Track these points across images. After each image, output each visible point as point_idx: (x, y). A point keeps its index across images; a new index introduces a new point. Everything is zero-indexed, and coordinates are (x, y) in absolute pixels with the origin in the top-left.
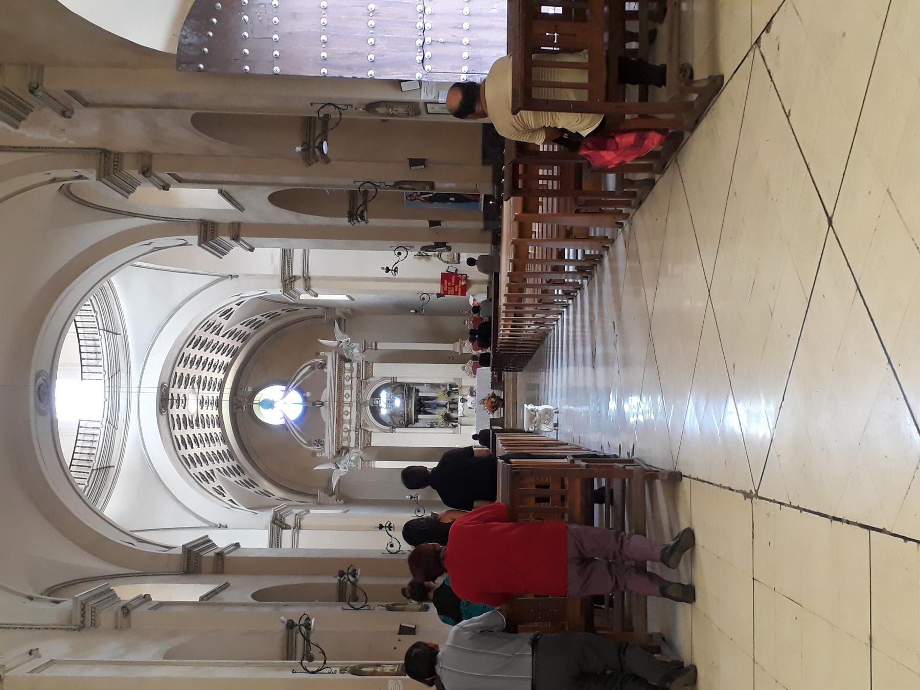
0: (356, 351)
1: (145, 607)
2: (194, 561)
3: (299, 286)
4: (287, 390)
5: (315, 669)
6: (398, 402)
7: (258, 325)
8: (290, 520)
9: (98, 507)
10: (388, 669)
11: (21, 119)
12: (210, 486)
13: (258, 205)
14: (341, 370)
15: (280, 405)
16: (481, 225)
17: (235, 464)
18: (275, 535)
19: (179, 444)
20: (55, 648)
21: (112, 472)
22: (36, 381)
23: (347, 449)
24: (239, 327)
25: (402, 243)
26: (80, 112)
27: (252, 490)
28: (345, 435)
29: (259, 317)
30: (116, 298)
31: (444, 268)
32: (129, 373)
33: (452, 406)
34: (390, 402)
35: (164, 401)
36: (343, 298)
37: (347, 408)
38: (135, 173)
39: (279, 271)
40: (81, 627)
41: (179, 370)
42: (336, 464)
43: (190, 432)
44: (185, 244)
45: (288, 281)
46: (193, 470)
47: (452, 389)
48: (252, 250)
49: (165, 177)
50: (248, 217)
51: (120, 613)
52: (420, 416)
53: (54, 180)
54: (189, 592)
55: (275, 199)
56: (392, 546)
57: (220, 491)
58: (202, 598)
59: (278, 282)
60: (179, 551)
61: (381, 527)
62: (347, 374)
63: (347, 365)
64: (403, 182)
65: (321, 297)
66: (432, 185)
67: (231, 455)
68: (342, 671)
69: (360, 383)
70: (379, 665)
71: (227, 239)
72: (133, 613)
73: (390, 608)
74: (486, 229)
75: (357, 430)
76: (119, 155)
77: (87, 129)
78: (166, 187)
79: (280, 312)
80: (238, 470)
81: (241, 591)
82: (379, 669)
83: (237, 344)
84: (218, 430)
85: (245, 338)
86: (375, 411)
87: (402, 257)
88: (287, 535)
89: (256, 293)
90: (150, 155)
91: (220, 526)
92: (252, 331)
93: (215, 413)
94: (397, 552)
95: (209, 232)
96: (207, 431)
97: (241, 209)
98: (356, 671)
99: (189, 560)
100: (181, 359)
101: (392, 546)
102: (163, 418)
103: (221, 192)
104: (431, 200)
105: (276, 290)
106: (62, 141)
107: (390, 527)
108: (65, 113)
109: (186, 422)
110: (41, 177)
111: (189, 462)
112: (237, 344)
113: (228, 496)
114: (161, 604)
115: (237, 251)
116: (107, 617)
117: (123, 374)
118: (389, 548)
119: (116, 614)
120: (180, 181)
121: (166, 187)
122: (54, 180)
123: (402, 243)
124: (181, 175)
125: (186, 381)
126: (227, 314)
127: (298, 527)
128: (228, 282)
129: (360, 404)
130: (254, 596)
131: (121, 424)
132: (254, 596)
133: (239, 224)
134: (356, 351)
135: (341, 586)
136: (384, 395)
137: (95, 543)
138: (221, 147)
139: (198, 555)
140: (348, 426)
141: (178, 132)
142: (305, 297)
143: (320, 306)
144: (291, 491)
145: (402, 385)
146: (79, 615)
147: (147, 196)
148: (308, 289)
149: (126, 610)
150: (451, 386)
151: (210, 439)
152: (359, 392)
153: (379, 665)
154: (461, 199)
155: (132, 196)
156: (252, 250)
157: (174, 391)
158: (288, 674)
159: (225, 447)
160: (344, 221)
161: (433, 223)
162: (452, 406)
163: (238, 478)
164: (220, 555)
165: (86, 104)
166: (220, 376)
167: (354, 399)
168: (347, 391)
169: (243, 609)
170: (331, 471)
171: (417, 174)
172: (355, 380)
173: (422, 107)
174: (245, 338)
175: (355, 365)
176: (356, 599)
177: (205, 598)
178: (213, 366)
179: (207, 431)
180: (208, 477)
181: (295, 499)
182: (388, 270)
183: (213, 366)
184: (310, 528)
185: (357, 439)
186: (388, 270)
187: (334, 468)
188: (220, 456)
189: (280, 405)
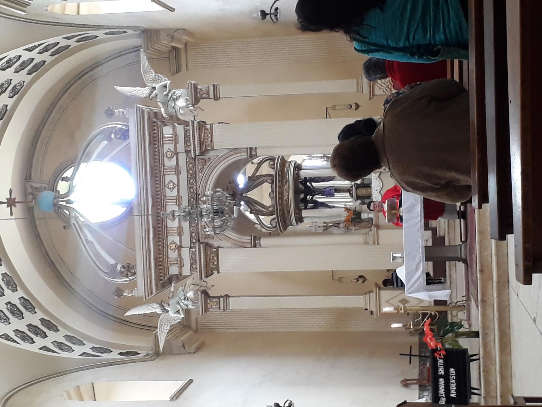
0: (181, 103)
28: (173, 254)
33: (363, 192)
42: (162, 306)
52: (305, 213)
69: (192, 162)
79: (72, 43)
134: (181, 103)
140: (177, 239)
143: (129, 27)
152: (192, 177)
162: (363, 192)
163: (16, 324)
168: (171, 177)
170: (156, 316)
172: (182, 157)
175: (180, 129)
187: (158, 310)
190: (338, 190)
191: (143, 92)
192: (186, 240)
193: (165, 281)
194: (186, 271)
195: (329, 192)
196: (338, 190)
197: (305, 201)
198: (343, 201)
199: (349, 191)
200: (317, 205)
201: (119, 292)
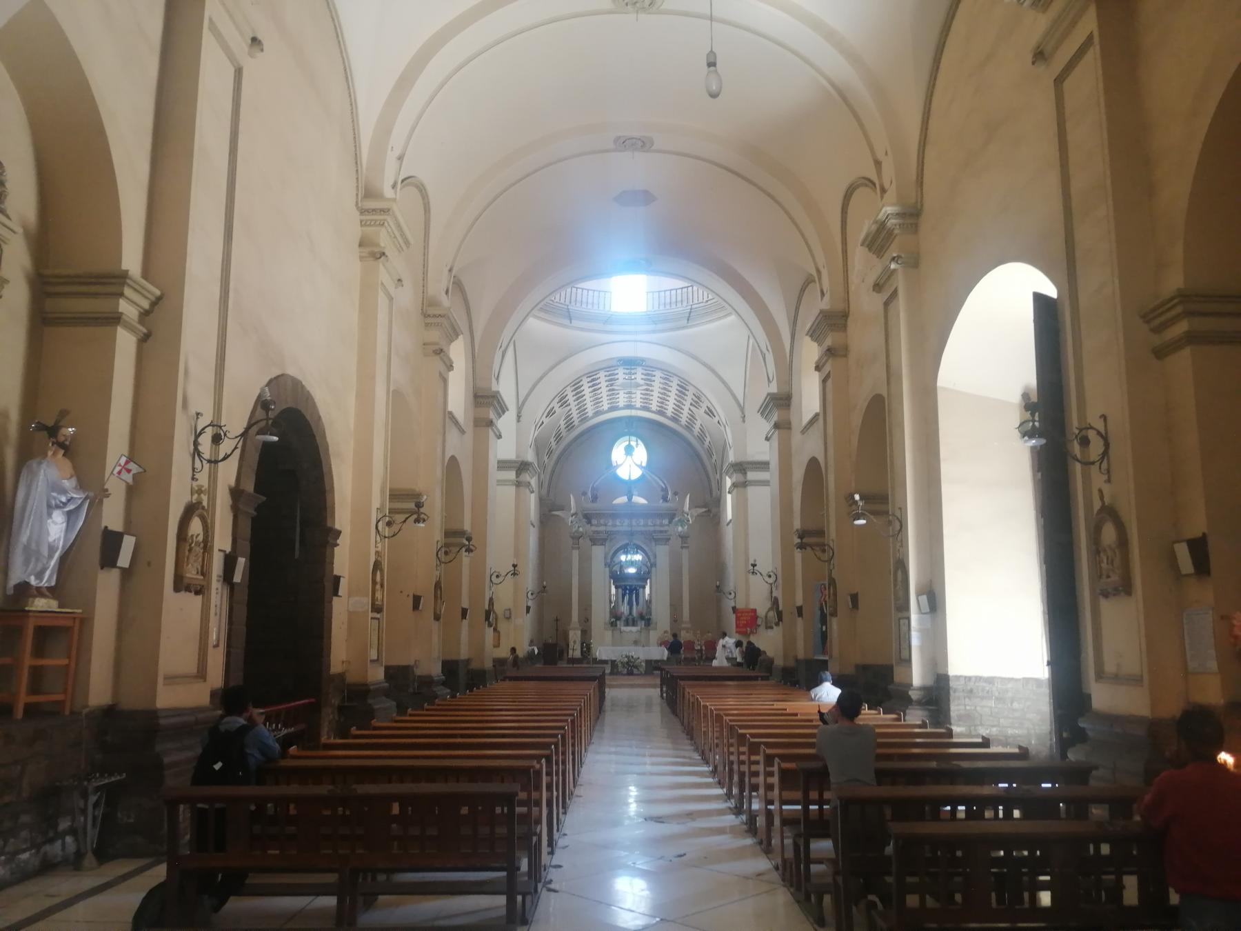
1: (443, 368)
2: (485, 401)
3: (737, 477)
4: (640, 466)
5: (380, 528)
6: (632, 570)
7: (701, 439)
8: (526, 477)
9: (535, 312)
10: (378, 595)
11: (870, 247)
12: (555, 405)
13: (809, 447)
14: (661, 516)
15: (629, 461)
16: (801, 655)
17: (576, 423)
19: (592, 375)
20: (406, 297)
21: (567, 322)
23: (589, 522)
24: (698, 423)
25: (780, 581)
26: (879, 299)
27: (552, 440)
28: (602, 521)
29: (708, 439)
30: (720, 318)
31: (761, 612)
32: (654, 332)
34: (632, 563)
35: (630, 363)
36: (729, 514)
37: (627, 522)
38: (828, 342)
39: (750, 459)
40: (425, 315)
41: (658, 374)
42: (575, 514)
43: (603, 385)
44: (769, 381)
45: (740, 468)
46: (569, 389)
47: (646, 619)
48: (767, 439)
49: (828, 368)
50: (796, 437)
51: (436, 347)
53: (818, 271)
54: (457, 399)
55: (813, 464)
57: (551, 413)
58: (450, 413)
59: (739, 460)
60: (494, 388)
61: (515, 566)
62: (658, 522)
63: (666, 522)
64: (835, 588)
65: (729, 497)
66: (834, 614)
67: (584, 419)
68: (377, 552)
70: (382, 586)
71: (775, 418)
72: (437, 357)
73: (438, 586)
74: (797, 660)
75: (607, 532)
76: (844, 328)
77: (866, 303)
78: (818, 368)
79: (715, 457)
80: (570, 426)
81: (457, 445)
82: (378, 587)
83: (684, 420)
84: (606, 407)
85: (689, 428)
86: (625, 549)
87: (767, 579)
88: (511, 475)
89: (730, 440)
90: (845, 356)
91: (519, 417)
92: (696, 433)
93: (621, 404)
95: (782, 401)
96: (605, 399)
97: (803, 432)
98: (377, 566)
99: (487, 397)
100: (668, 375)
102: (615, 363)
103: (817, 415)
104: (821, 609)
105: (732, 457)
106: (854, 279)
108: (878, 287)
109: (611, 380)
110: (821, 261)
111: (576, 386)
112: (684, 420)
113: (546, 421)
114: (445, 381)
115: (765, 426)
116: (434, 335)
117: (652, 327)
119: (437, 344)
120: (824, 381)
121: (818, 368)
122: (818, 271)
123: (780, 581)
124: (829, 382)
125: (649, 379)
126: (710, 412)
127: (518, 484)
128: (739, 413)
129: (632, 534)
130: (453, 458)
131: (609, 328)
132: (453, 458)
133: (790, 428)
134: (680, 529)
135: (462, 533)
136: (638, 557)
137: (500, 316)
138: (857, 420)
141: (869, 383)
142: (728, 482)
144: (553, 471)
145: (649, 572)
146: (437, 313)
147: (810, 351)
148: (734, 485)
149: (440, 352)
150: (649, 620)
151: (597, 401)
152: (642, 533)
153: (382, 586)
154: (824, 636)
155: (808, 339)
156: (767, 439)
157: (639, 370)
158: (376, 503)
159: (590, 414)
160: (797, 524)
161: (800, 611)
163: (563, 427)
164: (490, 423)
165: (886, 304)
166: (654, 408)
167: (634, 529)
169: (439, 450)
171: (844, 602)
172: (652, 529)
173: (904, 614)
174: (689, 428)
175: (666, 528)
176: (446, 553)
177: (451, 416)
178: (663, 400)
179: (605, 399)
180: (563, 402)
181: (546, 478)
182: (754, 565)
183: (663, 400)
184: (517, 492)
185: (598, 532)
186: (754, 565)
187: (573, 511)
188: (582, 410)
189: (629, 461)
190: (631, 609)
191: (686, 508)
192: (609, 529)
193: (588, 518)
194: (594, 528)
195: (630, 603)
196: (631, 609)
197: (625, 589)
198: (624, 609)
199: (631, 613)
200: (623, 596)
201: (584, 494)
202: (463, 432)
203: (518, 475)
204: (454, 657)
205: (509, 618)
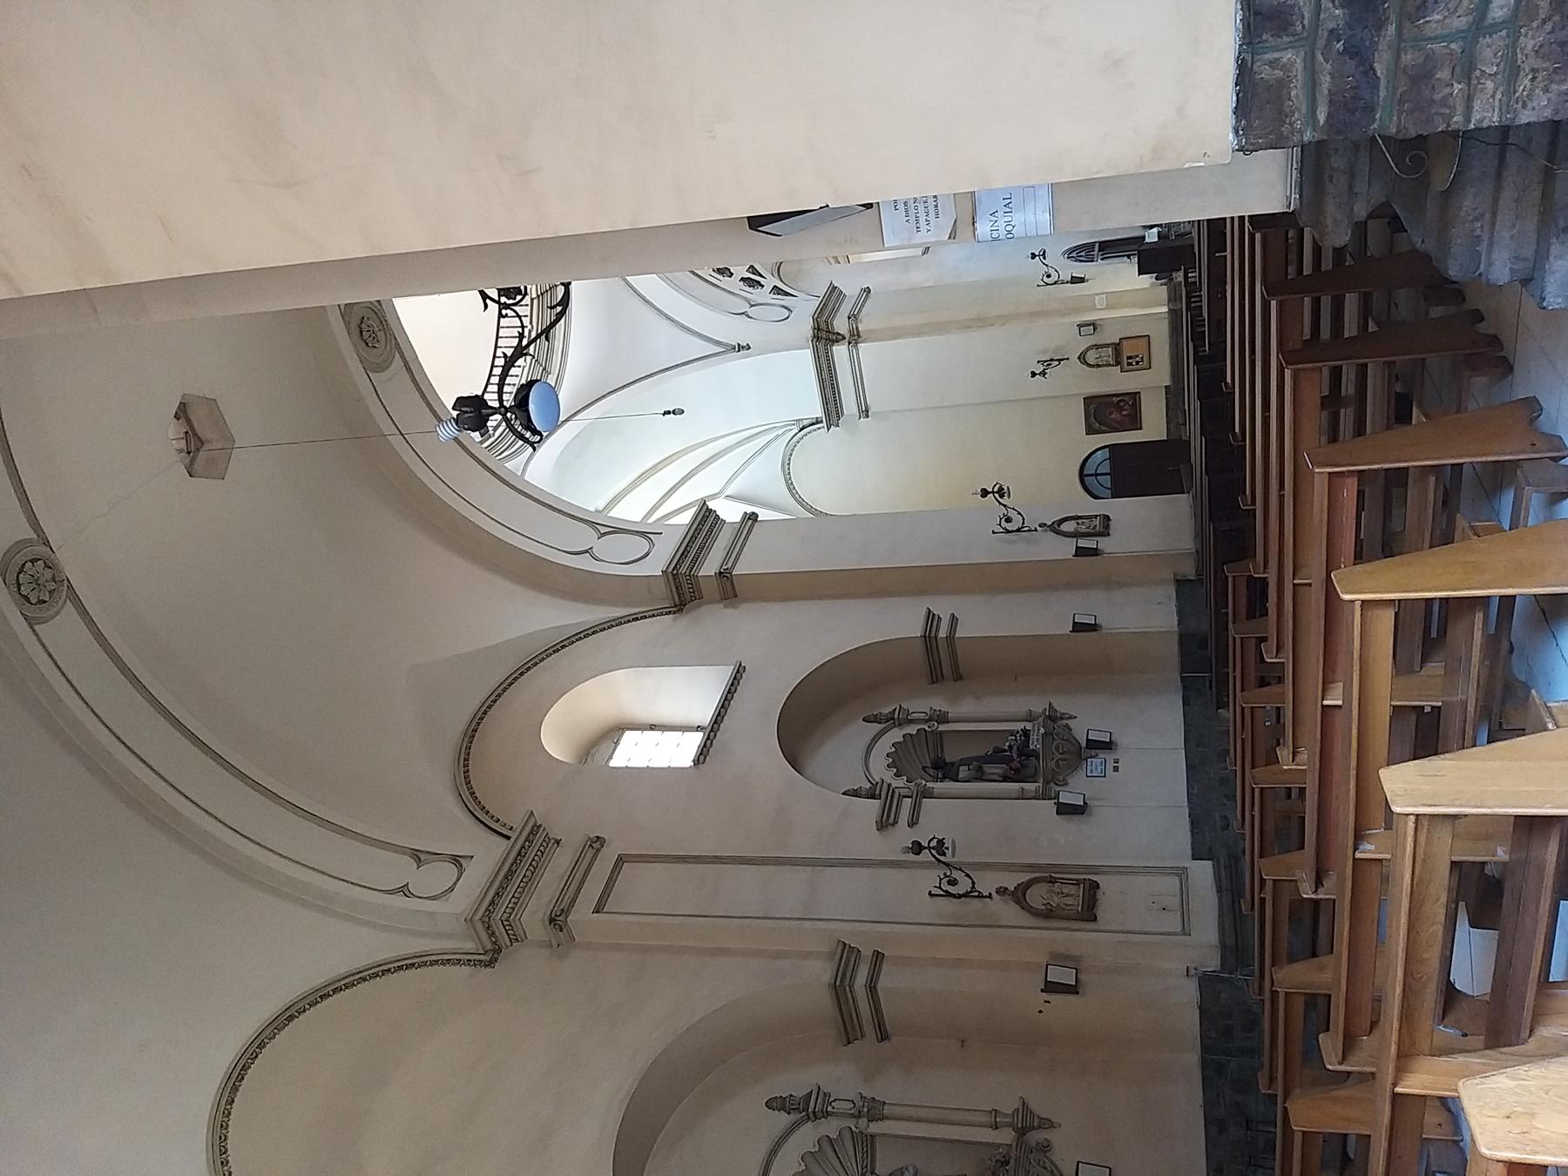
8: (841, 325)
18: (822, 353)
22: (347, 324)
56: (1008, 520)
58: (697, 762)
61: (985, 493)
88: (840, 351)
94: (1018, 530)
101: (1008, 520)
107: (1001, 492)
118: (1004, 524)
127: (855, 338)
137: (536, 575)
139: (693, 579)
202: (739, 672)
203: (838, 338)
204: (1176, 637)
205: (1094, 324)
